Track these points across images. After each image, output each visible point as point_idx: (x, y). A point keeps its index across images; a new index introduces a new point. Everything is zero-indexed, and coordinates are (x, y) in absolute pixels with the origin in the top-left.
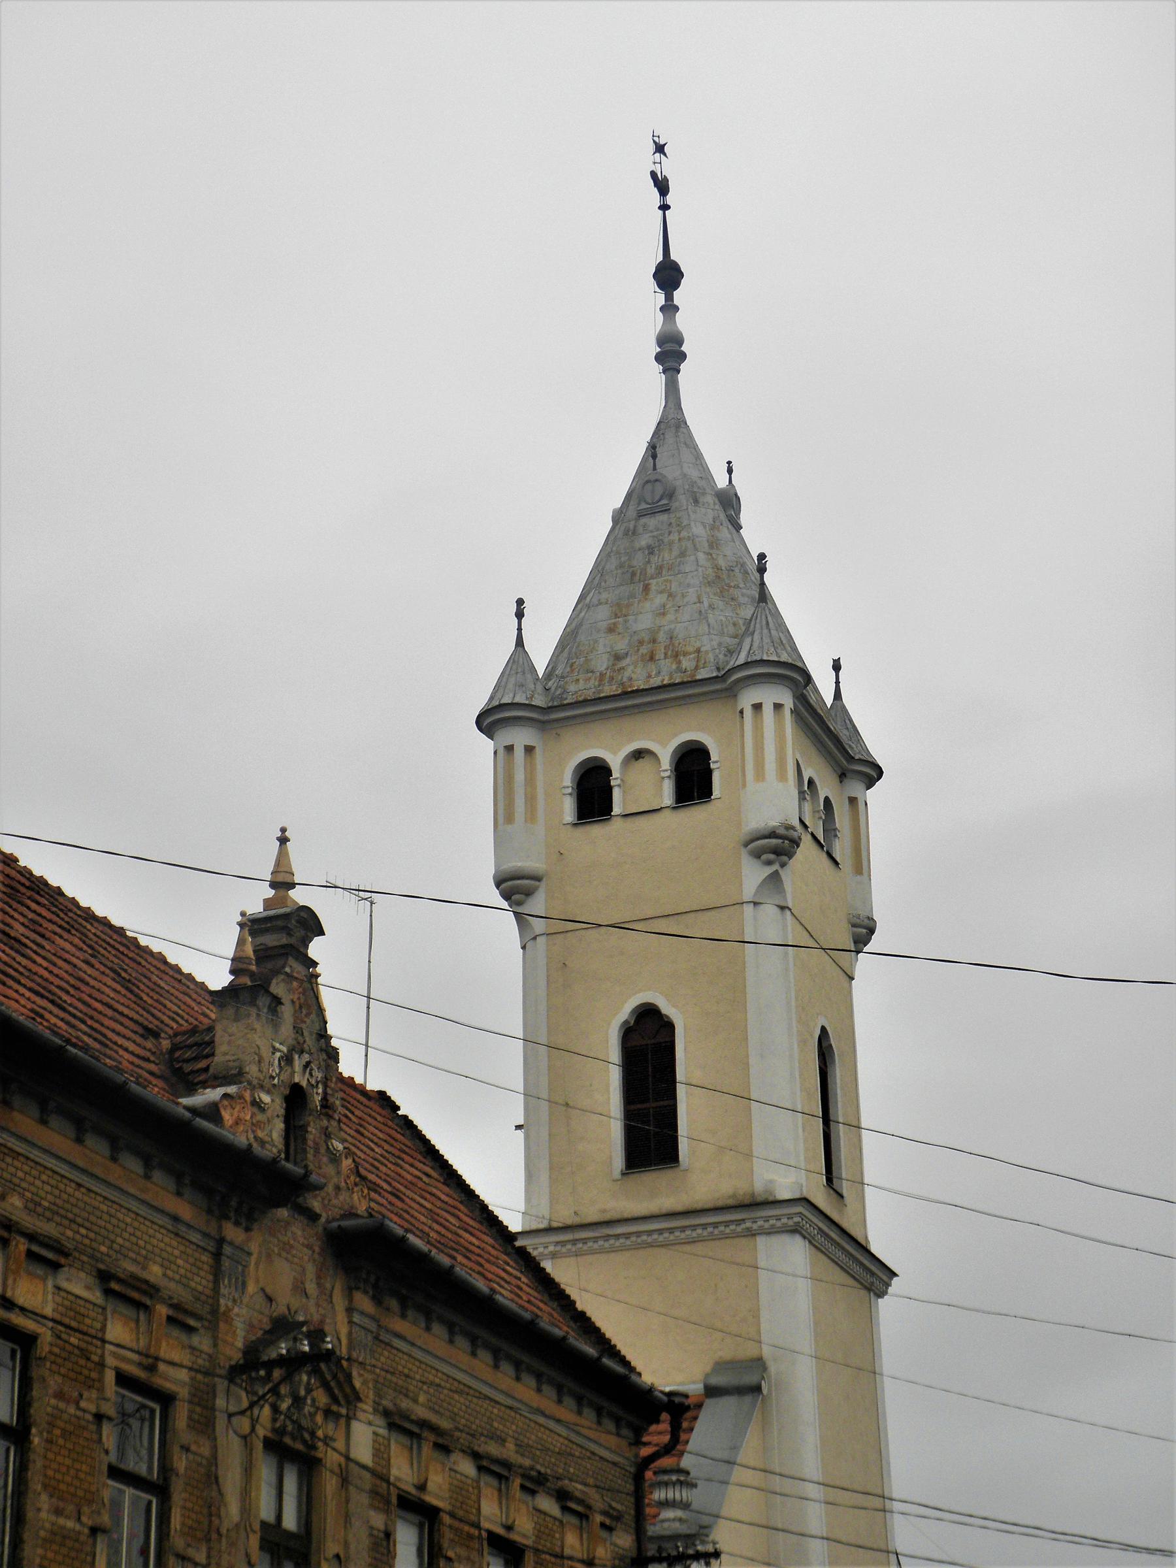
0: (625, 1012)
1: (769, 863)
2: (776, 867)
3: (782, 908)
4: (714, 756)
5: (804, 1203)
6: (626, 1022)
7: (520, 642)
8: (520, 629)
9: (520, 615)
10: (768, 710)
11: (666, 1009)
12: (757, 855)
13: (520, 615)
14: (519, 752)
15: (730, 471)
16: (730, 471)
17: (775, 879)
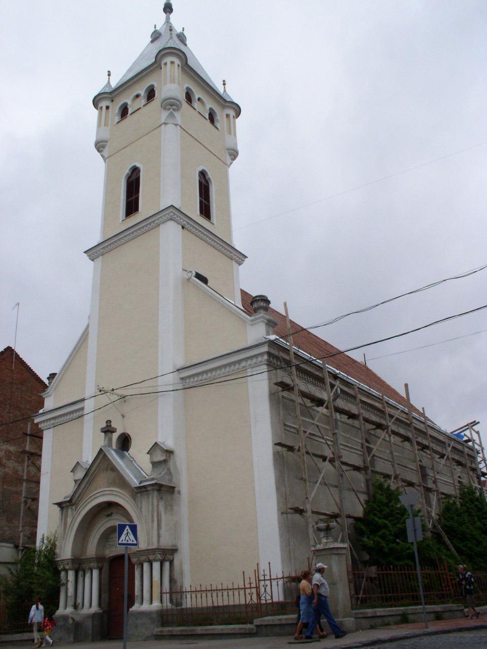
0: (127, 171)
1: (169, 109)
5: (172, 207)
6: (128, 174)
7: (109, 82)
9: (109, 75)
10: (169, 64)
11: (138, 165)
12: (165, 109)
13: (109, 75)
14: (104, 108)
15: (183, 30)
16: (183, 30)
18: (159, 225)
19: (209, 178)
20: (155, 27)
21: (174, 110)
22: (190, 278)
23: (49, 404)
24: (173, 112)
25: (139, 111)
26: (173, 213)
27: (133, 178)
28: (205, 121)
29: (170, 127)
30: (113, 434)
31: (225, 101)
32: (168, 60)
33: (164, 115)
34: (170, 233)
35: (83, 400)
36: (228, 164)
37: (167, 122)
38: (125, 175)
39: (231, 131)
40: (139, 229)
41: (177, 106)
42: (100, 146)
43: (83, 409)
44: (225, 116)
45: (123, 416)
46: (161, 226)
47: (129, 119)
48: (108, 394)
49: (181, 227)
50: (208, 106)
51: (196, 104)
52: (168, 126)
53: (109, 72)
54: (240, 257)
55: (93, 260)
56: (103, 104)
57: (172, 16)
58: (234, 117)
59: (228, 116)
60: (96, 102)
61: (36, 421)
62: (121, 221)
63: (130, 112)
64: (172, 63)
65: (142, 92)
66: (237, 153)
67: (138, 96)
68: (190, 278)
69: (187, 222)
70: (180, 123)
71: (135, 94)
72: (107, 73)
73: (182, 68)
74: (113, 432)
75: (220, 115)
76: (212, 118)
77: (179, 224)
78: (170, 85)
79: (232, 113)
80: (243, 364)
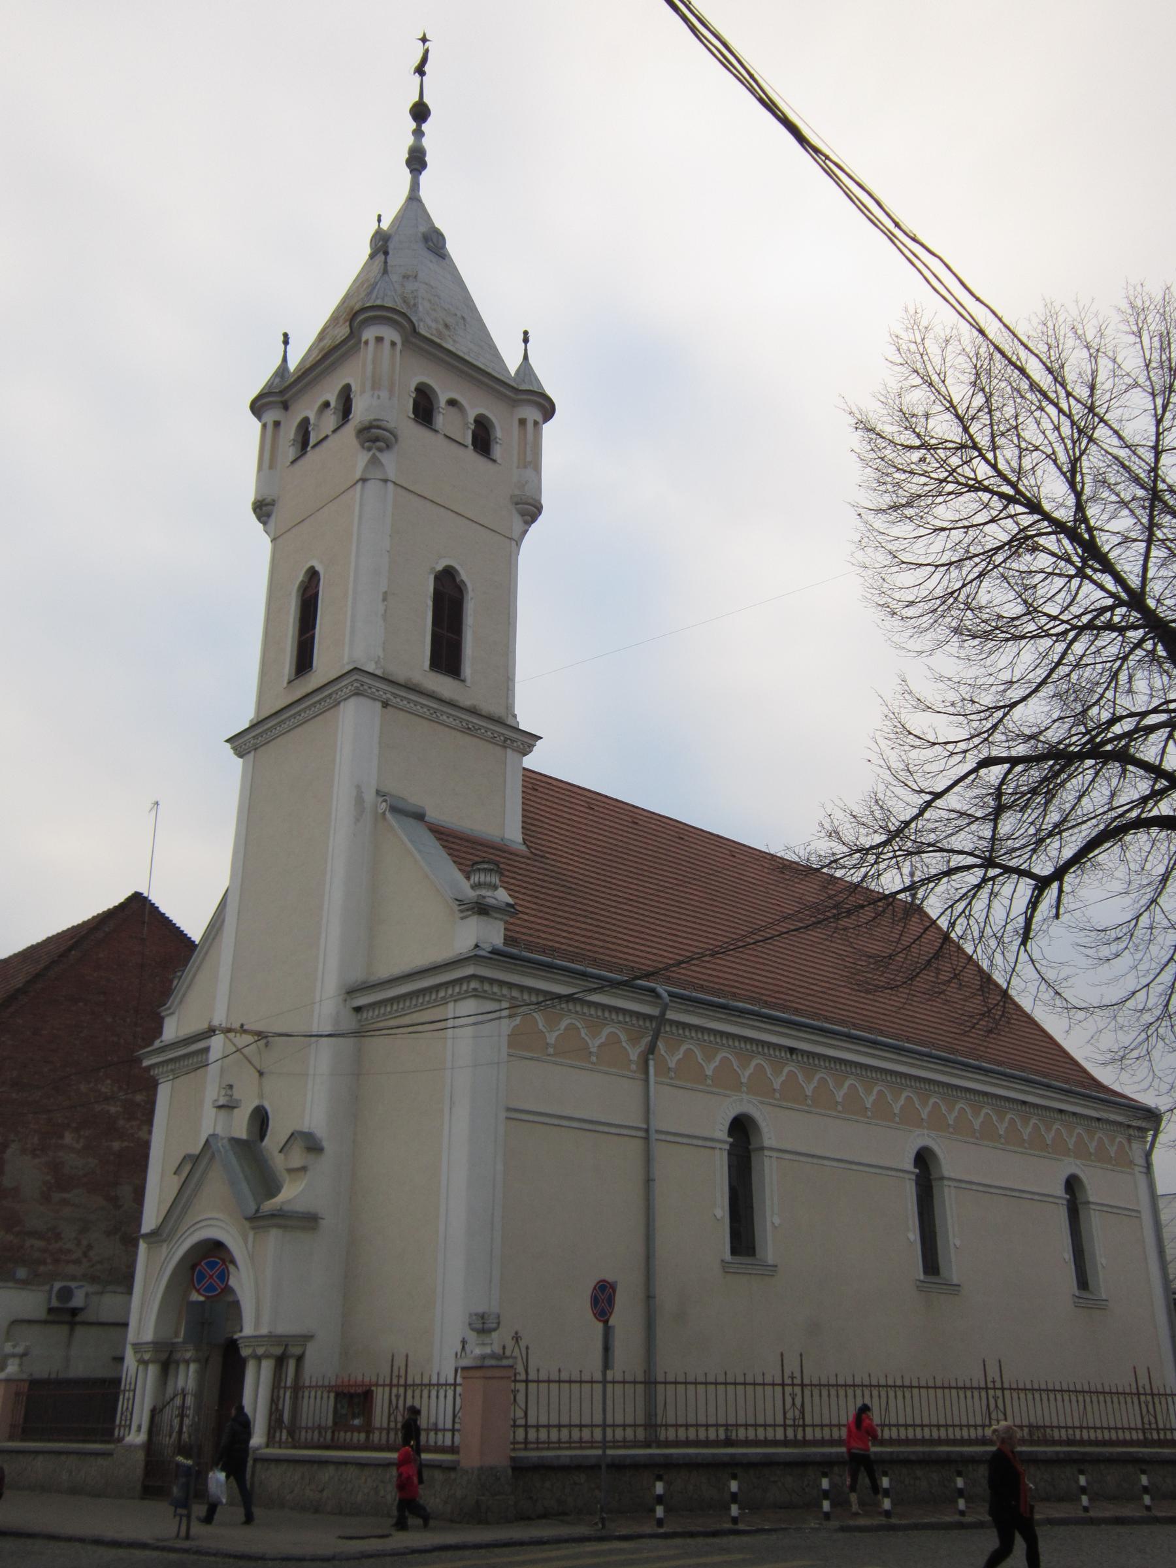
1: (369, 449)
2: (374, 451)
3: (386, 481)
4: (353, 388)
6: (302, 582)
7: (285, 359)
8: (285, 352)
13: (286, 342)
17: (374, 462)
18: (339, 703)
19: (462, 581)
20: (379, 220)
21: (380, 450)
22: (384, 813)
23: (171, 1030)
24: (378, 454)
25: (325, 444)
26: (358, 681)
27: (311, 592)
28: (460, 451)
30: (236, 1111)
32: (369, 334)
33: (363, 458)
34: (355, 720)
35: (211, 1031)
36: (515, 536)
37: (368, 476)
38: (297, 583)
39: (531, 459)
40: (309, 707)
41: (384, 440)
42: (263, 509)
43: (207, 1050)
44: (516, 423)
45: (261, 1074)
46: (342, 704)
48: (231, 1035)
49: (378, 705)
50: (471, 416)
51: (444, 418)
52: (369, 484)
53: (286, 335)
54: (528, 741)
55: (241, 756)
56: (270, 416)
57: (424, 177)
58: (536, 423)
59: (522, 422)
60: (257, 407)
61: (146, 1063)
62: (285, 684)
63: (312, 442)
64: (379, 340)
65: (332, 398)
66: (539, 509)
67: (327, 404)
68: (384, 813)
69: (393, 694)
70: (391, 475)
72: (282, 338)
73: (406, 342)
74: (234, 1108)
76: (483, 439)
77: (375, 699)
79: (531, 414)
80: (442, 994)
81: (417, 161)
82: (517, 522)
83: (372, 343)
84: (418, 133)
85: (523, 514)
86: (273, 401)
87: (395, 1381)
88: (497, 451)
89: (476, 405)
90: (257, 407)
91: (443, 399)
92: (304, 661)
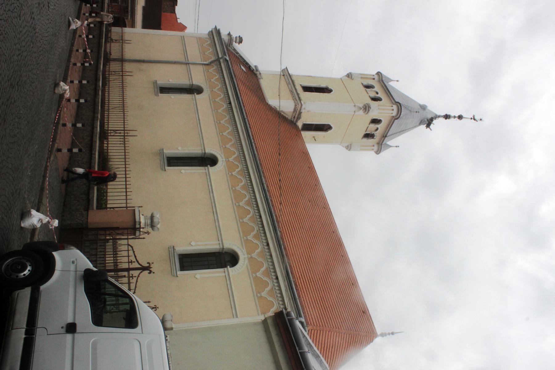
0: (330, 87)
11: (332, 93)
14: (373, 77)
29: (354, 109)
31: (381, 144)
32: (395, 107)
33: (361, 106)
39: (364, 148)
42: (349, 76)
47: (364, 89)
51: (373, 126)
56: (376, 77)
60: (379, 74)
63: (368, 90)
64: (393, 110)
65: (379, 95)
67: (377, 93)
70: (356, 113)
71: (378, 91)
73: (393, 117)
75: (370, 141)
76: (368, 136)
78: (383, 111)
81: (447, 117)
82: (346, 145)
83: (392, 108)
84: (455, 117)
85: (348, 146)
86: (381, 78)
87: (126, 132)
88: (365, 140)
89: (378, 134)
90: (379, 74)
91: (378, 126)
92: (307, 89)
